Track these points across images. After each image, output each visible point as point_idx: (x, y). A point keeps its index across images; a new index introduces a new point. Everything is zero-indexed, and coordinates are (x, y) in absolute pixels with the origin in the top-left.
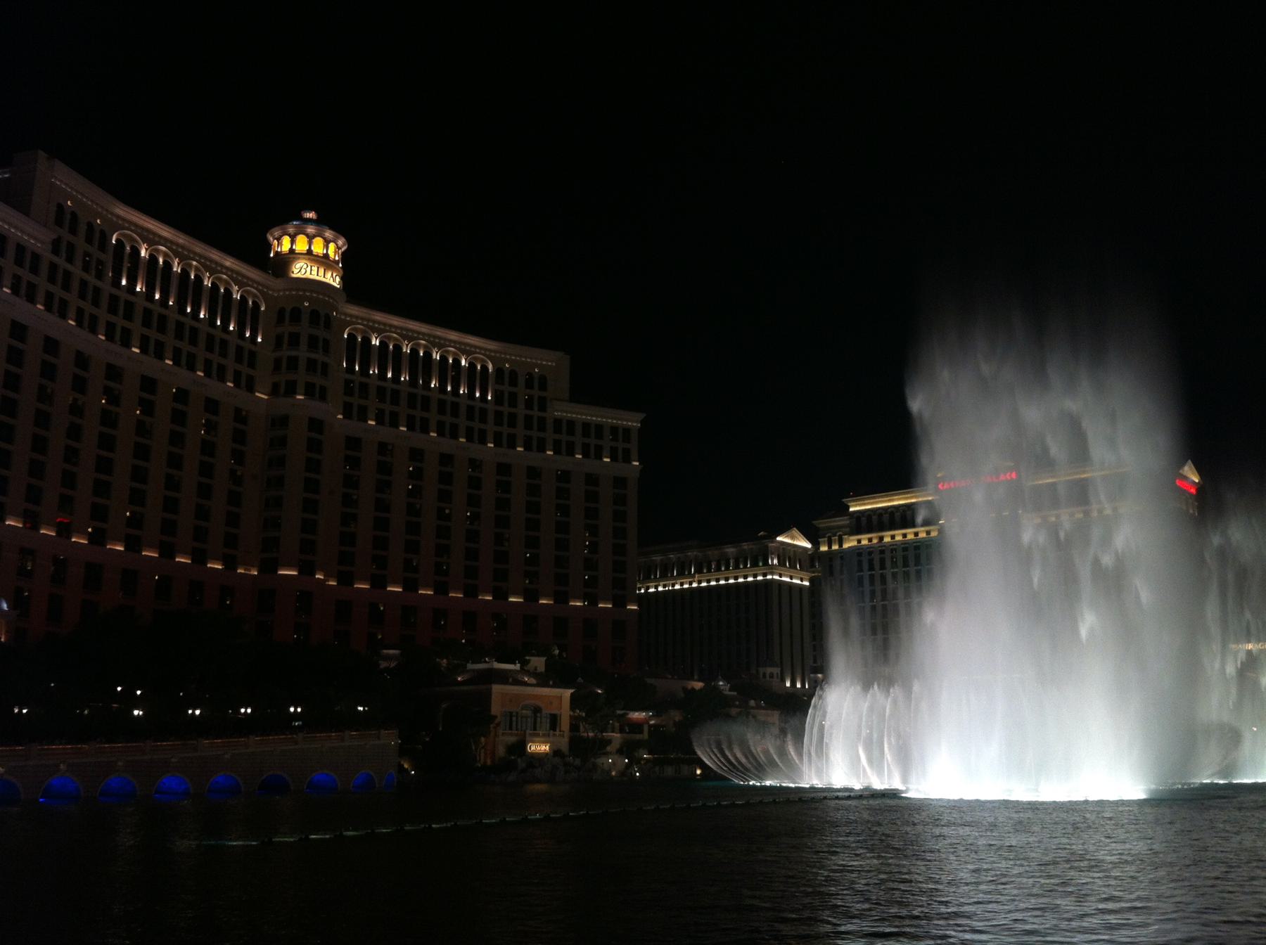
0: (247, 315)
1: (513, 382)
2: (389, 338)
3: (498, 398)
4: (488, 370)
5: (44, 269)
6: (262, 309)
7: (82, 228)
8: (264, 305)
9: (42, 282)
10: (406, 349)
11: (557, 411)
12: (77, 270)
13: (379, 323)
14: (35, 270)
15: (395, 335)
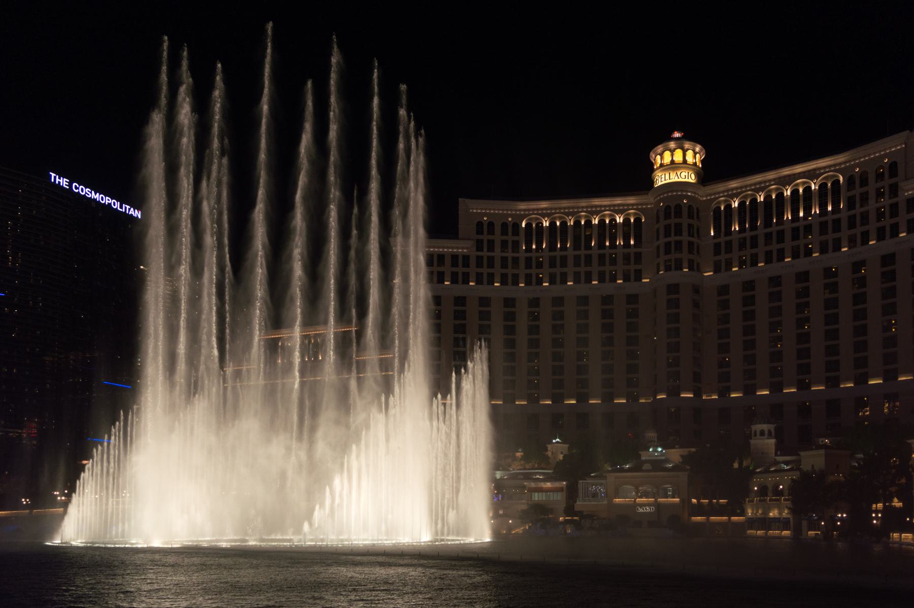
0: (633, 229)
1: (864, 181)
2: (746, 197)
3: (851, 204)
4: (839, 181)
5: (473, 262)
6: (643, 221)
7: (498, 229)
8: (643, 217)
9: (473, 270)
10: (761, 198)
11: (908, 191)
12: (497, 253)
13: (737, 188)
14: (466, 264)
15: (750, 192)
